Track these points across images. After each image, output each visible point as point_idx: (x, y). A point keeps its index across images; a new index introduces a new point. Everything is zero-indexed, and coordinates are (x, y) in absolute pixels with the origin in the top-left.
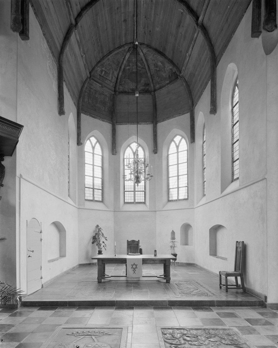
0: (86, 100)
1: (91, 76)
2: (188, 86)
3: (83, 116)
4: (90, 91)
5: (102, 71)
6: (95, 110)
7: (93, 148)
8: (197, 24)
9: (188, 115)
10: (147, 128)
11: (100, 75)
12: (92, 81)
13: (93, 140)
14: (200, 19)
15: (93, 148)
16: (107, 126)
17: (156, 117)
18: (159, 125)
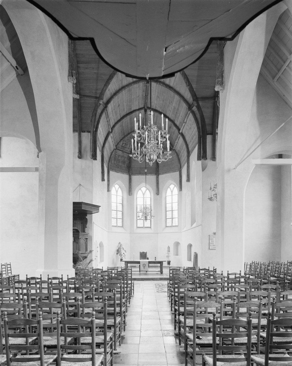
0: (113, 162)
1: (117, 148)
2: (178, 155)
3: (111, 172)
4: (115, 156)
5: (123, 144)
6: (118, 167)
7: (117, 192)
8: (179, 133)
9: (178, 173)
10: (152, 178)
11: (122, 146)
12: (117, 150)
13: (117, 186)
14: (181, 131)
15: (117, 192)
16: (126, 177)
17: (158, 171)
18: (160, 176)
